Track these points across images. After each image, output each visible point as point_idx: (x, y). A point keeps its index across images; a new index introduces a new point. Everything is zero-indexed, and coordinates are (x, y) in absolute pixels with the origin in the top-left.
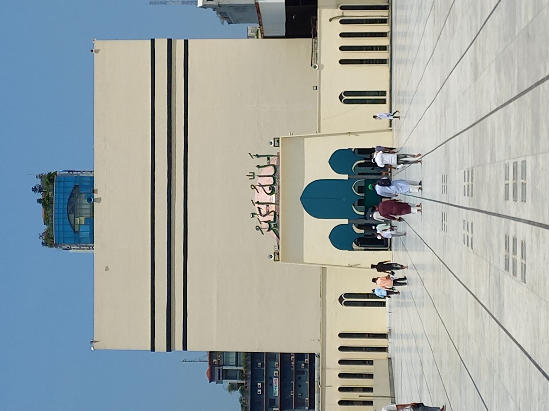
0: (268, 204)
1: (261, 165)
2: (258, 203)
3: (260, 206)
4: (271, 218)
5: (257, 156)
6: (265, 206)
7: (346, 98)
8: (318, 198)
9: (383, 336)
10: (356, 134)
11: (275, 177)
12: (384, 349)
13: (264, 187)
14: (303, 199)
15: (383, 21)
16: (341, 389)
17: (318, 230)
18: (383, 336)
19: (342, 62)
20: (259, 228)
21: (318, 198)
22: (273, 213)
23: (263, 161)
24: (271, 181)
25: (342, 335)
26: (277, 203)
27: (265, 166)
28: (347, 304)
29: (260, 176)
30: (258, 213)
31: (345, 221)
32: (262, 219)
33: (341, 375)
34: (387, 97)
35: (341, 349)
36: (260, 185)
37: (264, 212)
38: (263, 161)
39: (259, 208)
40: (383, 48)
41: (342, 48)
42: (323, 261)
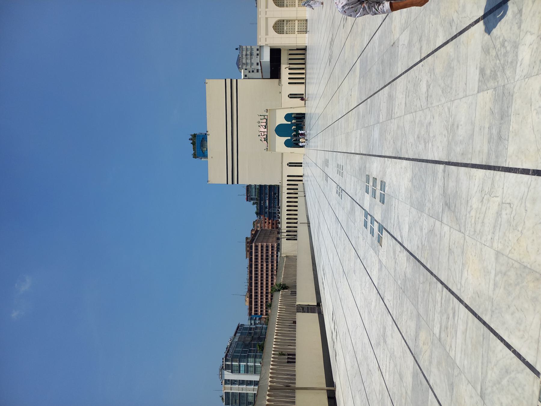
8: (281, 130)
9: (301, 176)
10: (293, 108)
11: (266, 123)
12: (301, 181)
16: (288, 193)
17: (280, 141)
18: (301, 176)
19: (289, 83)
20: (261, 140)
21: (281, 130)
23: (263, 117)
25: (288, 176)
26: (267, 132)
28: (290, 166)
31: (290, 138)
33: (288, 189)
35: (288, 180)
38: (263, 117)
40: (303, 78)
41: (289, 78)
42: (282, 152)
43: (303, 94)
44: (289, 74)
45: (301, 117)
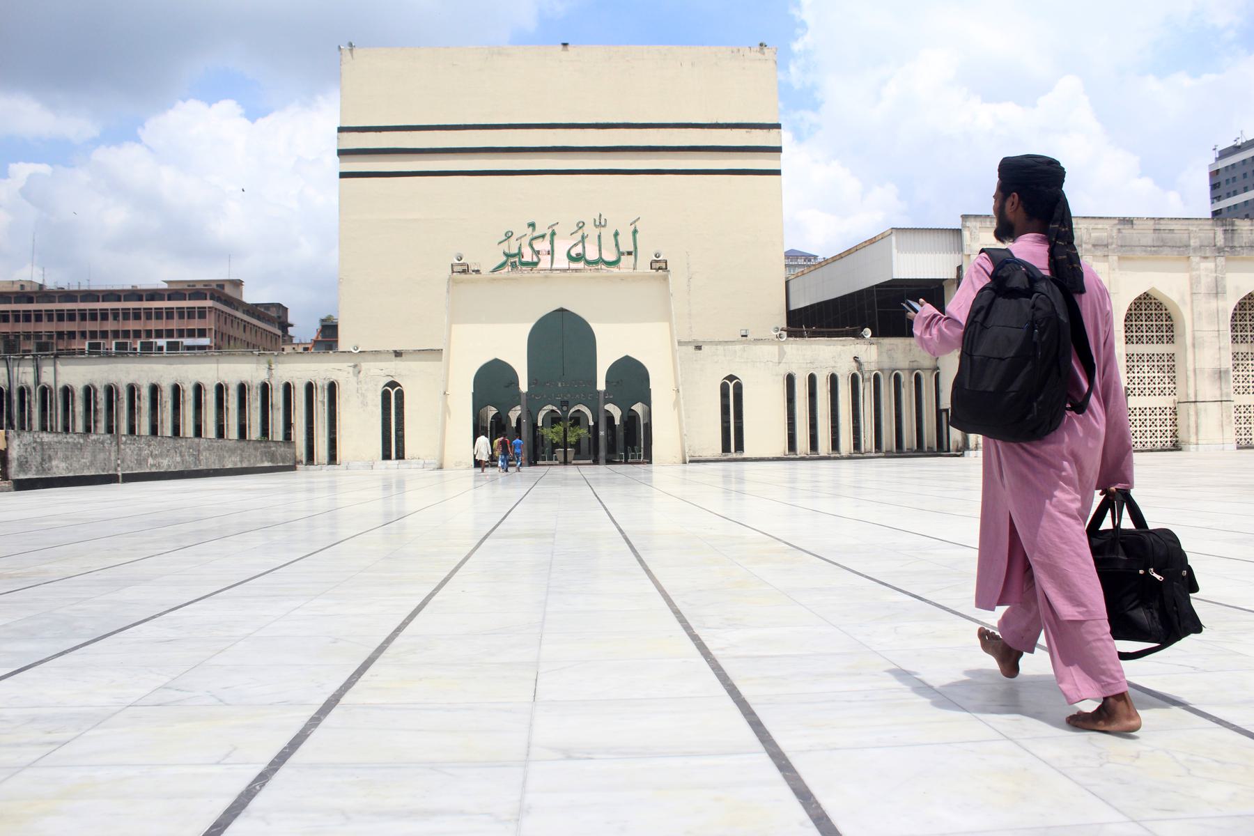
0: (551, 253)
1: (619, 238)
2: (553, 234)
3: (548, 237)
4: (528, 257)
5: (635, 232)
6: (548, 248)
7: (731, 386)
8: (561, 338)
13: (580, 246)
14: (562, 311)
15: (857, 446)
19: (790, 380)
20: (509, 236)
21: (561, 338)
22: (535, 260)
23: (626, 245)
24: (592, 254)
27: (617, 245)
29: (599, 237)
30: (536, 234)
31: (524, 386)
32: (525, 241)
34: (733, 455)
36: (583, 237)
37: (538, 245)
39: (543, 236)
41: (812, 379)
43: (740, 447)
44: (834, 380)
45: (627, 442)
